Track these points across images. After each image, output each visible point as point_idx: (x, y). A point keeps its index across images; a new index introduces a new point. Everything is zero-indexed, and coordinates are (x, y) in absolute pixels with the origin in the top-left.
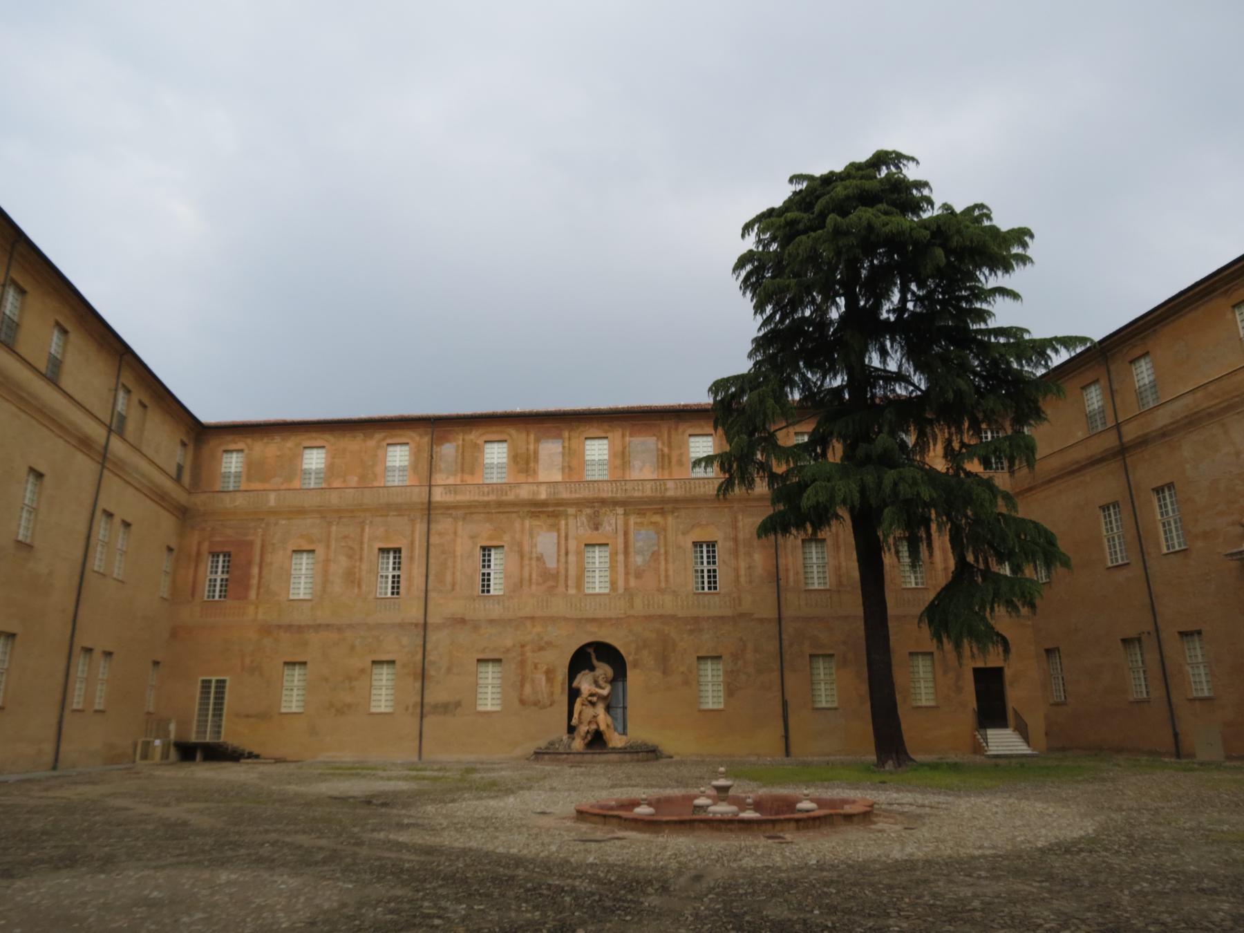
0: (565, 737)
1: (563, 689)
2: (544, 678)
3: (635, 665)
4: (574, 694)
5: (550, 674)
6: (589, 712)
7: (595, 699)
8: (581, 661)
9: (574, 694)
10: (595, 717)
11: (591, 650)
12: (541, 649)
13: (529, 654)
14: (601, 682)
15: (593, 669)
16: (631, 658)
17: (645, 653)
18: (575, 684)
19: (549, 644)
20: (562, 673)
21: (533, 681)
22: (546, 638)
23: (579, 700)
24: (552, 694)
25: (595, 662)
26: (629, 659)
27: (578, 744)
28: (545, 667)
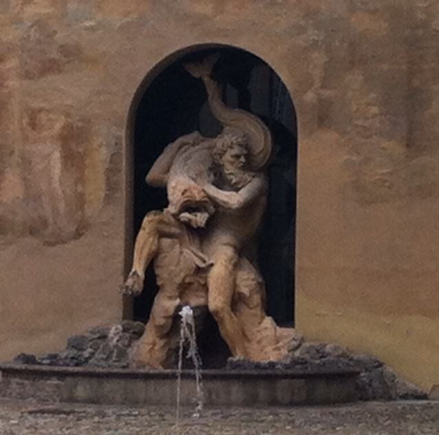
0: (115, 330)
1: (111, 187)
2: (57, 155)
3: (323, 118)
4: (147, 198)
5: (73, 142)
6: (180, 258)
7: (200, 219)
8: (171, 103)
9: (147, 198)
10: (201, 271)
11: (201, 72)
12: (50, 67)
13: (13, 83)
14: (231, 170)
15: (214, 129)
16: (310, 96)
17: (354, 80)
18: (153, 174)
19: (72, 53)
20: (109, 140)
21: (26, 163)
22: (60, 37)
23: (149, 221)
24: (80, 201)
25: (216, 105)
26: (305, 99)
27: (147, 349)
28: (58, 126)
